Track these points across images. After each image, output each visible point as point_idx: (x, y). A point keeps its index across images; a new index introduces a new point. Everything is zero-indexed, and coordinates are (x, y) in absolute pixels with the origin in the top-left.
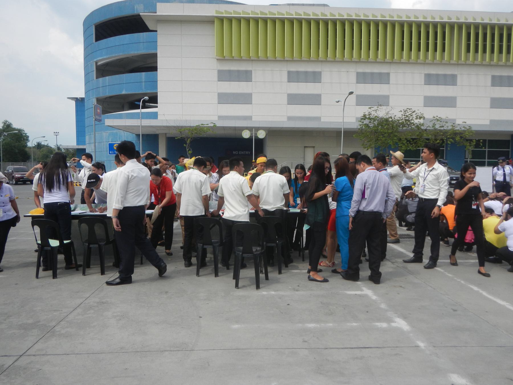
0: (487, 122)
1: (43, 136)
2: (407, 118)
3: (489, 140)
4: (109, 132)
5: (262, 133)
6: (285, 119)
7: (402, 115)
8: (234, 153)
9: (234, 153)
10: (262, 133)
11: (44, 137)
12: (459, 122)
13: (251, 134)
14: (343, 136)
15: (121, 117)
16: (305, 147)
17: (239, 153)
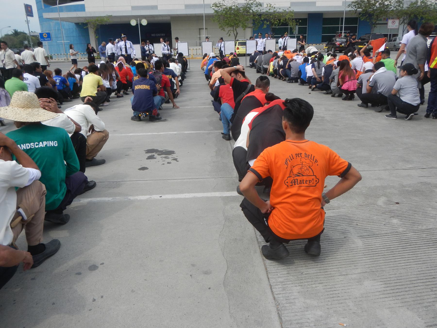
0: (340, 4)
1: (10, 26)
2: (248, 6)
3: (341, 18)
4: (55, 21)
5: (144, 21)
6: (183, 7)
7: (245, 3)
8: (152, 35)
9: (152, 35)
10: (144, 21)
11: (10, 27)
12: (318, 4)
13: (137, 22)
14: (205, 20)
15: (61, 10)
16: (200, 29)
17: (156, 35)
